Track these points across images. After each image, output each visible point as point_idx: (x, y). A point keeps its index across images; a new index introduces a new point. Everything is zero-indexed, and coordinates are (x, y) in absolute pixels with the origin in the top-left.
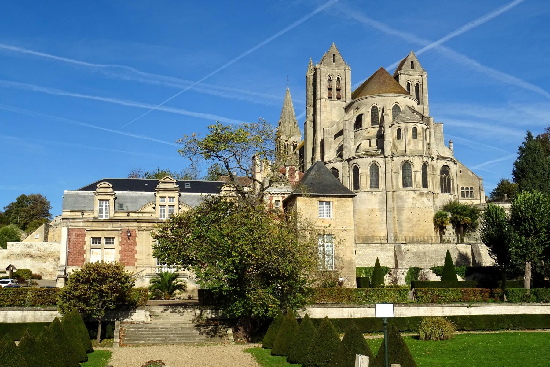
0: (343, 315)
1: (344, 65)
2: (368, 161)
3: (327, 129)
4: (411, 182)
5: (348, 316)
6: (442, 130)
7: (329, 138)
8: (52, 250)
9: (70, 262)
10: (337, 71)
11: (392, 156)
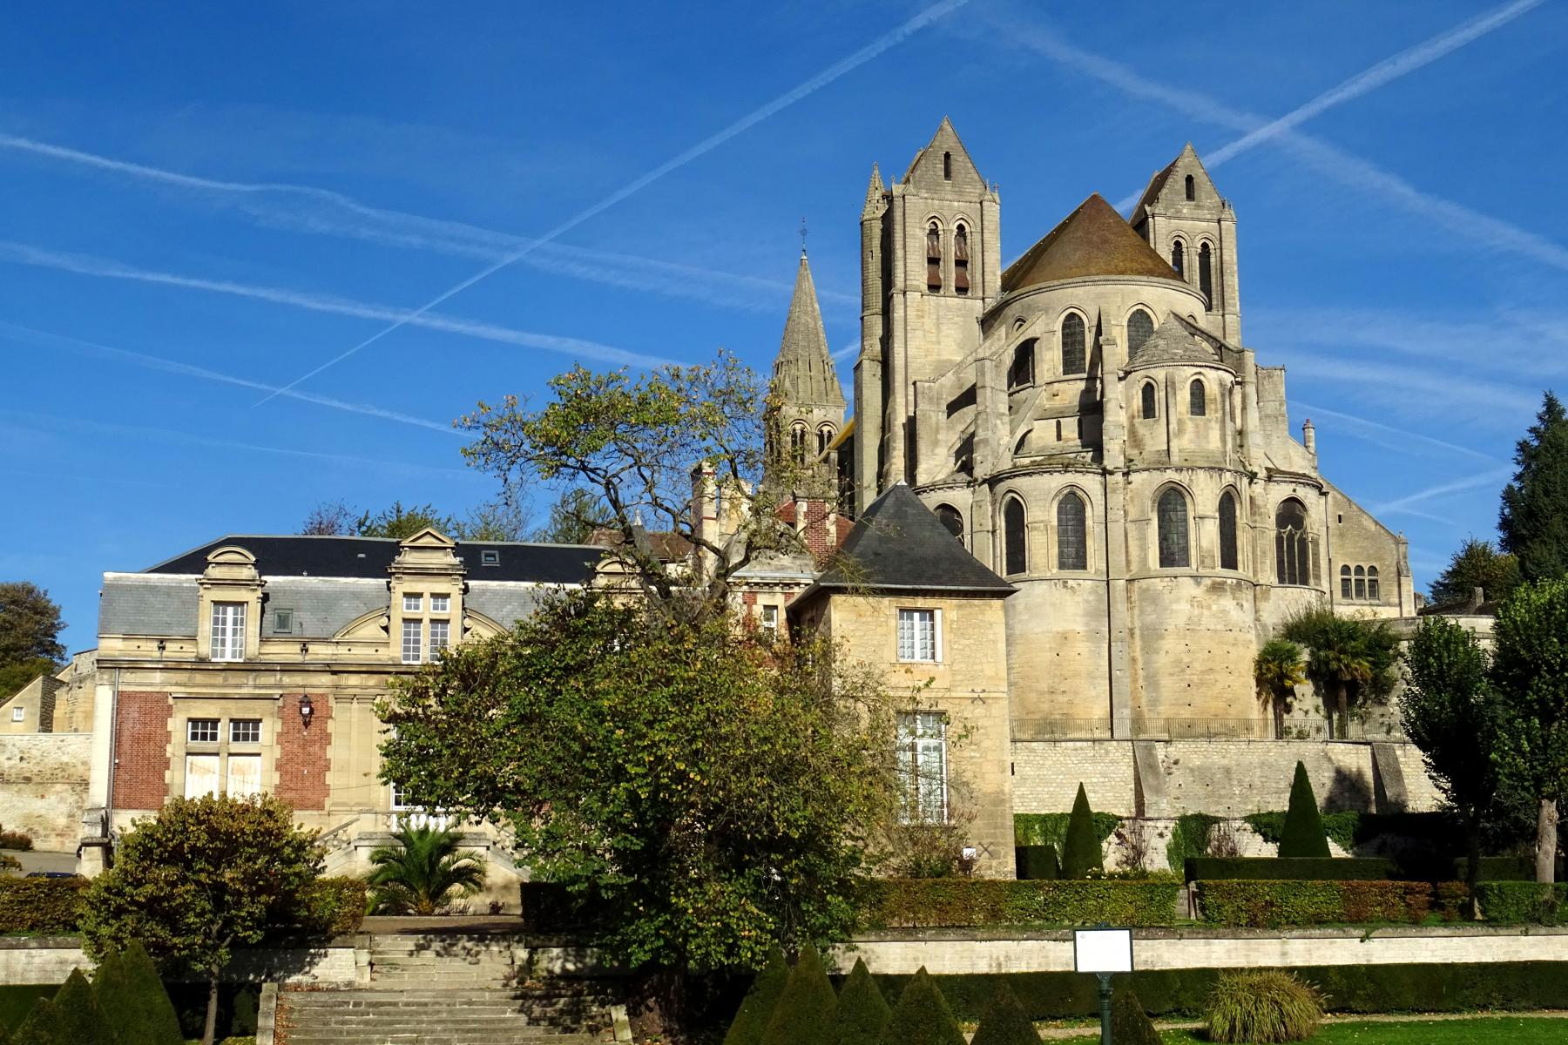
0: (973, 965)
1: (980, 186)
2: (1053, 485)
3: (927, 385)
4: (1185, 550)
5: (991, 966)
6: (1283, 390)
7: (932, 413)
8: (65, 759)
9: (121, 797)
10: (956, 204)
11: (1126, 470)
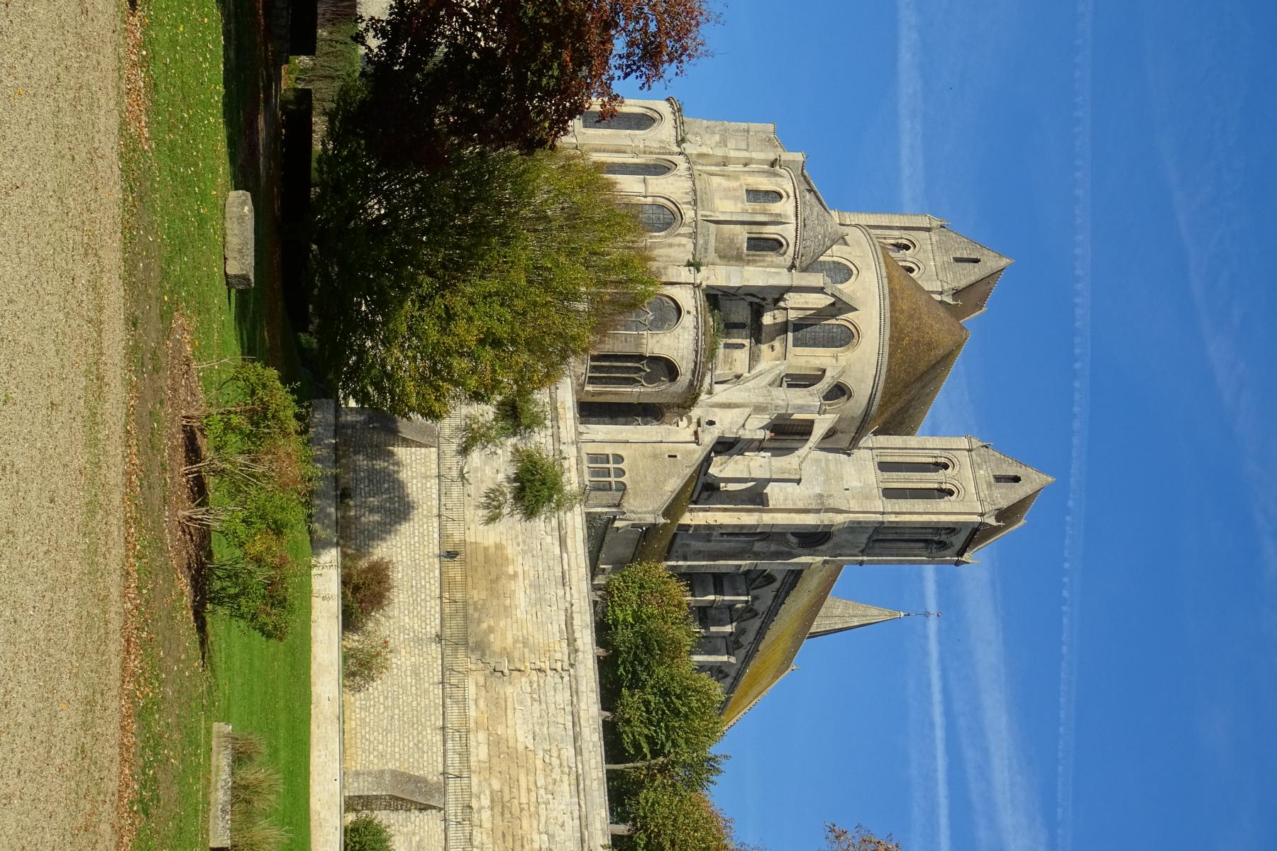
10: (932, 263)
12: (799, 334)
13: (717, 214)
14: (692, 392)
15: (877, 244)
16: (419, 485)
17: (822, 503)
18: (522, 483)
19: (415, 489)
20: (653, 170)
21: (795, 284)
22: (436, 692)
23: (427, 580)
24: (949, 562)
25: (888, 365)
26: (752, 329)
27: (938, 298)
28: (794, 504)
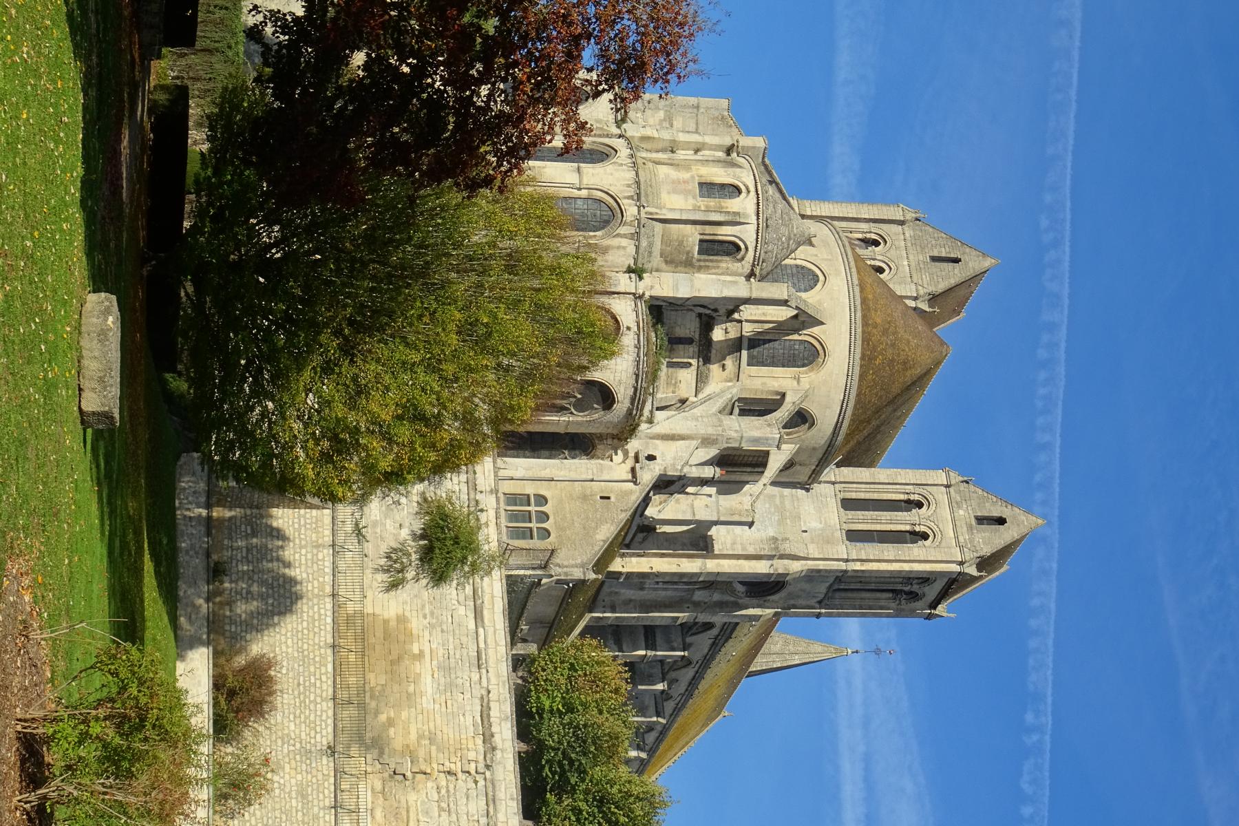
10: (906, 263)
12: (755, 351)
13: (664, 211)
14: (631, 422)
15: (844, 239)
16: (309, 556)
17: (776, 548)
18: (430, 541)
19: (303, 562)
20: (589, 156)
21: (754, 295)
22: (327, 818)
23: (318, 677)
24: (919, 616)
25: (858, 388)
26: (700, 345)
27: (912, 304)
28: (744, 549)
